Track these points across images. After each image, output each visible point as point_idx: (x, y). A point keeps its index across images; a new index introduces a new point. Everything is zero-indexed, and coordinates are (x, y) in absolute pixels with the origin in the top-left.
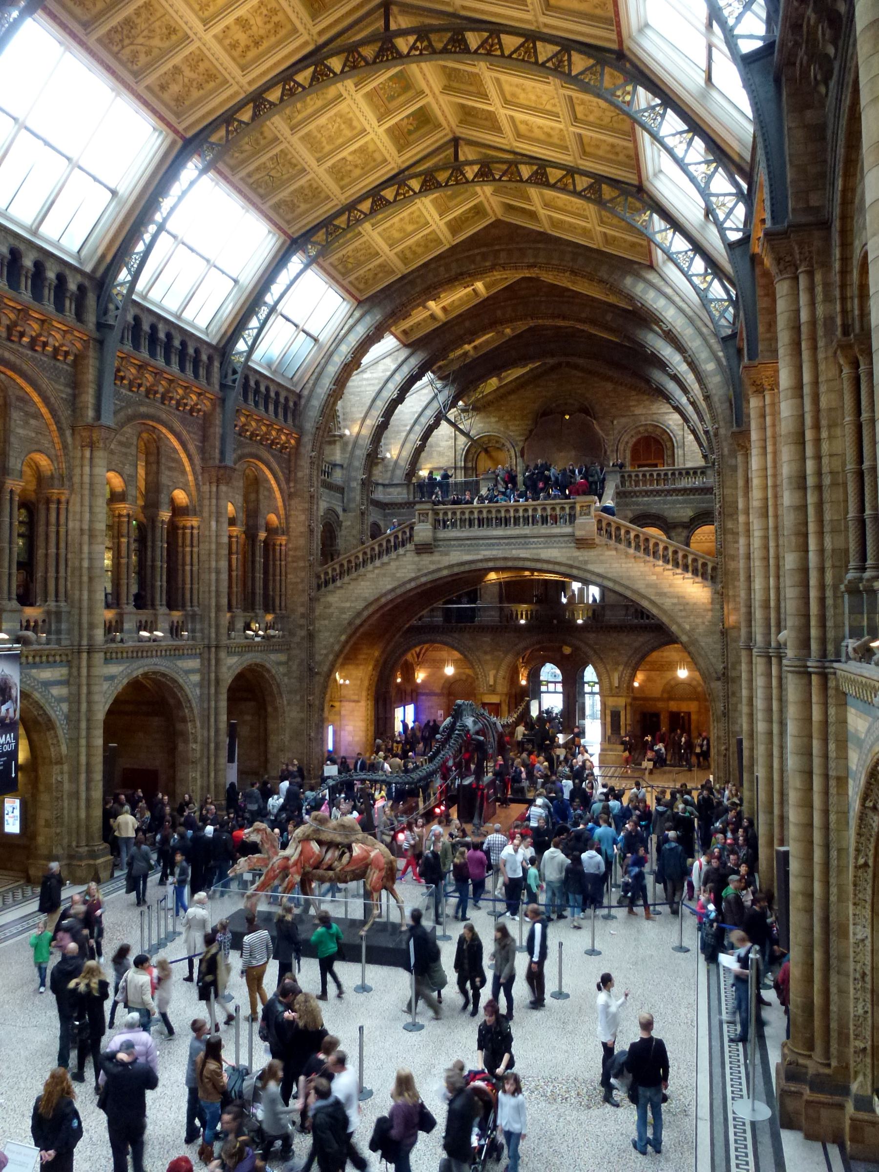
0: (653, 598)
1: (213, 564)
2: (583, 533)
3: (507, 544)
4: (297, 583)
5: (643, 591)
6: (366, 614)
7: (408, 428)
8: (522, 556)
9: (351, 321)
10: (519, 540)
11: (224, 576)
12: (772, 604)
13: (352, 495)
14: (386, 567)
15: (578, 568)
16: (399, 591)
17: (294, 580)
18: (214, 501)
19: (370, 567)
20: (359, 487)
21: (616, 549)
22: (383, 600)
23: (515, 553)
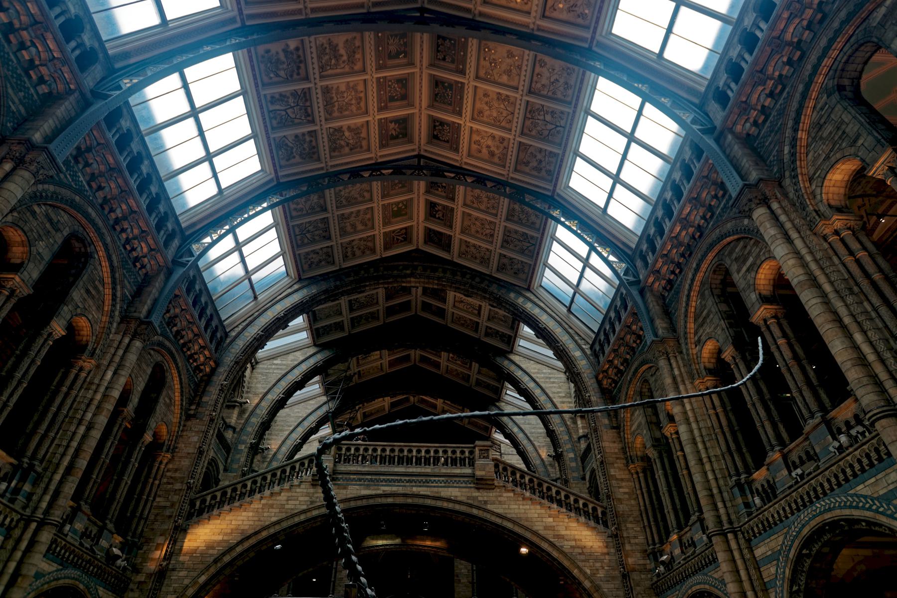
0: (552, 540)
1: (89, 416)
2: (483, 473)
3: (409, 481)
4: (165, 507)
5: (541, 532)
6: (239, 549)
7: (291, 428)
8: (422, 493)
9: (290, 291)
10: (420, 478)
11: (96, 434)
12: (871, 358)
13: (238, 456)
14: (274, 498)
15: (479, 508)
16: (285, 525)
17: (163, 504)
18: (120, 352)
19: (258, 496)
20: (246, 450)
21: (513, 491)
22: (264, 534)
23: (415, 489)
